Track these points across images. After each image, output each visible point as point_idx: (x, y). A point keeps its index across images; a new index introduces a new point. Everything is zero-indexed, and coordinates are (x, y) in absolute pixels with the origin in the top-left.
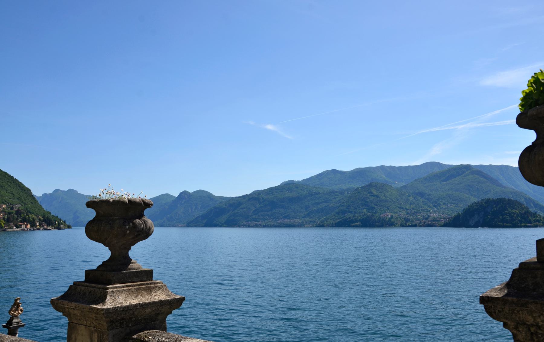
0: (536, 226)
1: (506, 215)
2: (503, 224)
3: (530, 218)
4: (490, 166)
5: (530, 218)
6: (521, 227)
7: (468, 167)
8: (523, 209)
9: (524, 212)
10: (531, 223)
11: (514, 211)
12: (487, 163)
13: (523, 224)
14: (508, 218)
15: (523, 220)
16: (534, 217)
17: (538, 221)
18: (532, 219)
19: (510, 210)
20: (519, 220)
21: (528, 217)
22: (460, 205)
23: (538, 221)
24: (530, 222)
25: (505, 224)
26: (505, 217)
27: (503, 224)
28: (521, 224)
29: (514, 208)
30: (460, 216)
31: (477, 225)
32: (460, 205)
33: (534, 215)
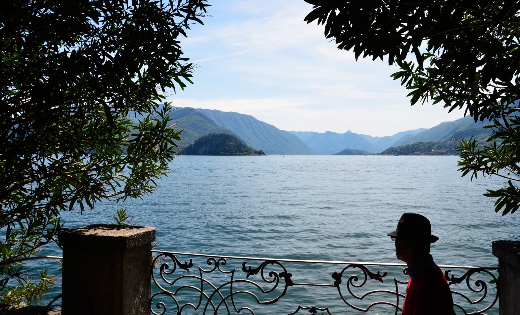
0: (246, 155)
1: (226, 146)
2: (224, 153)
3: (242, 149)
4: (207, 109)
5: (242, 149)
6: (236, 155)
7: (191, 110)
8: (237, 142)
9: (238, 144)
10: (243, 153)
11: (231, 143)
13: (237, 153)
14: (228, 149)
15: (237, 150)
16: (245, 148)
17: (247, 151)
18: (243, 150)
19: (228, 142)
20: (235, 150)
21: (241, 148)
22: (186, 138)
23: (247, 151)
24: (242, 152)
25: (225, 153)
26: (225, 148)
27: (224, 153)
28: (236, 153)
29: (231, 142)
30: (192, 146)
31: (205, 153)
32: (186, 138)
33: (244, 146)
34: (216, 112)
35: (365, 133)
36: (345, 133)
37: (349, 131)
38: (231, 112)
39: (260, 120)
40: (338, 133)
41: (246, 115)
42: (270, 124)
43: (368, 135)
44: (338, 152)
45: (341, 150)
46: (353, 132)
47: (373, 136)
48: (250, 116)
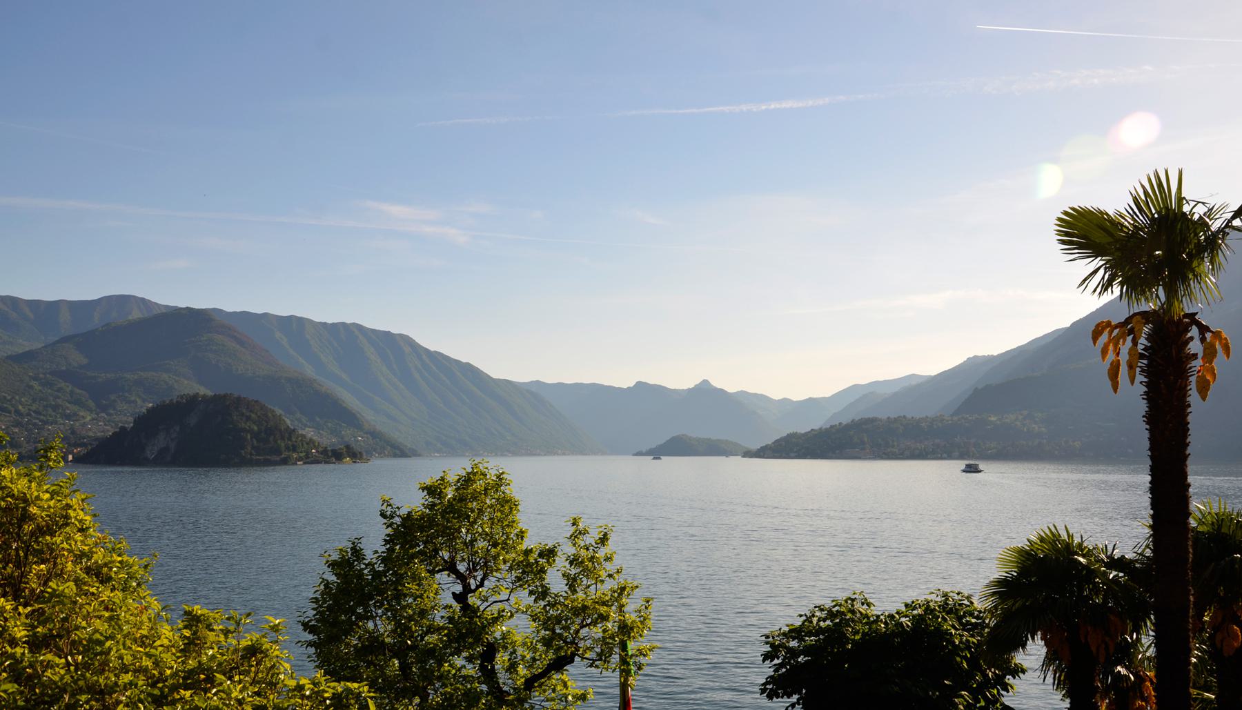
4: (265, 315)
12: (258, 309)
34: (294, 326)
35: (752, 389)
36: (692, 386)
37: (705, 382)
38: (344, 324)
39: (432, 349)
40: (672, 387)
41: (388, 334)
42: (464, 361)
43: (762, 395)
44: (654, 446)
45: (661, 440)
46: (717, 384)
47: (776, 395)
48: (401, 335)
